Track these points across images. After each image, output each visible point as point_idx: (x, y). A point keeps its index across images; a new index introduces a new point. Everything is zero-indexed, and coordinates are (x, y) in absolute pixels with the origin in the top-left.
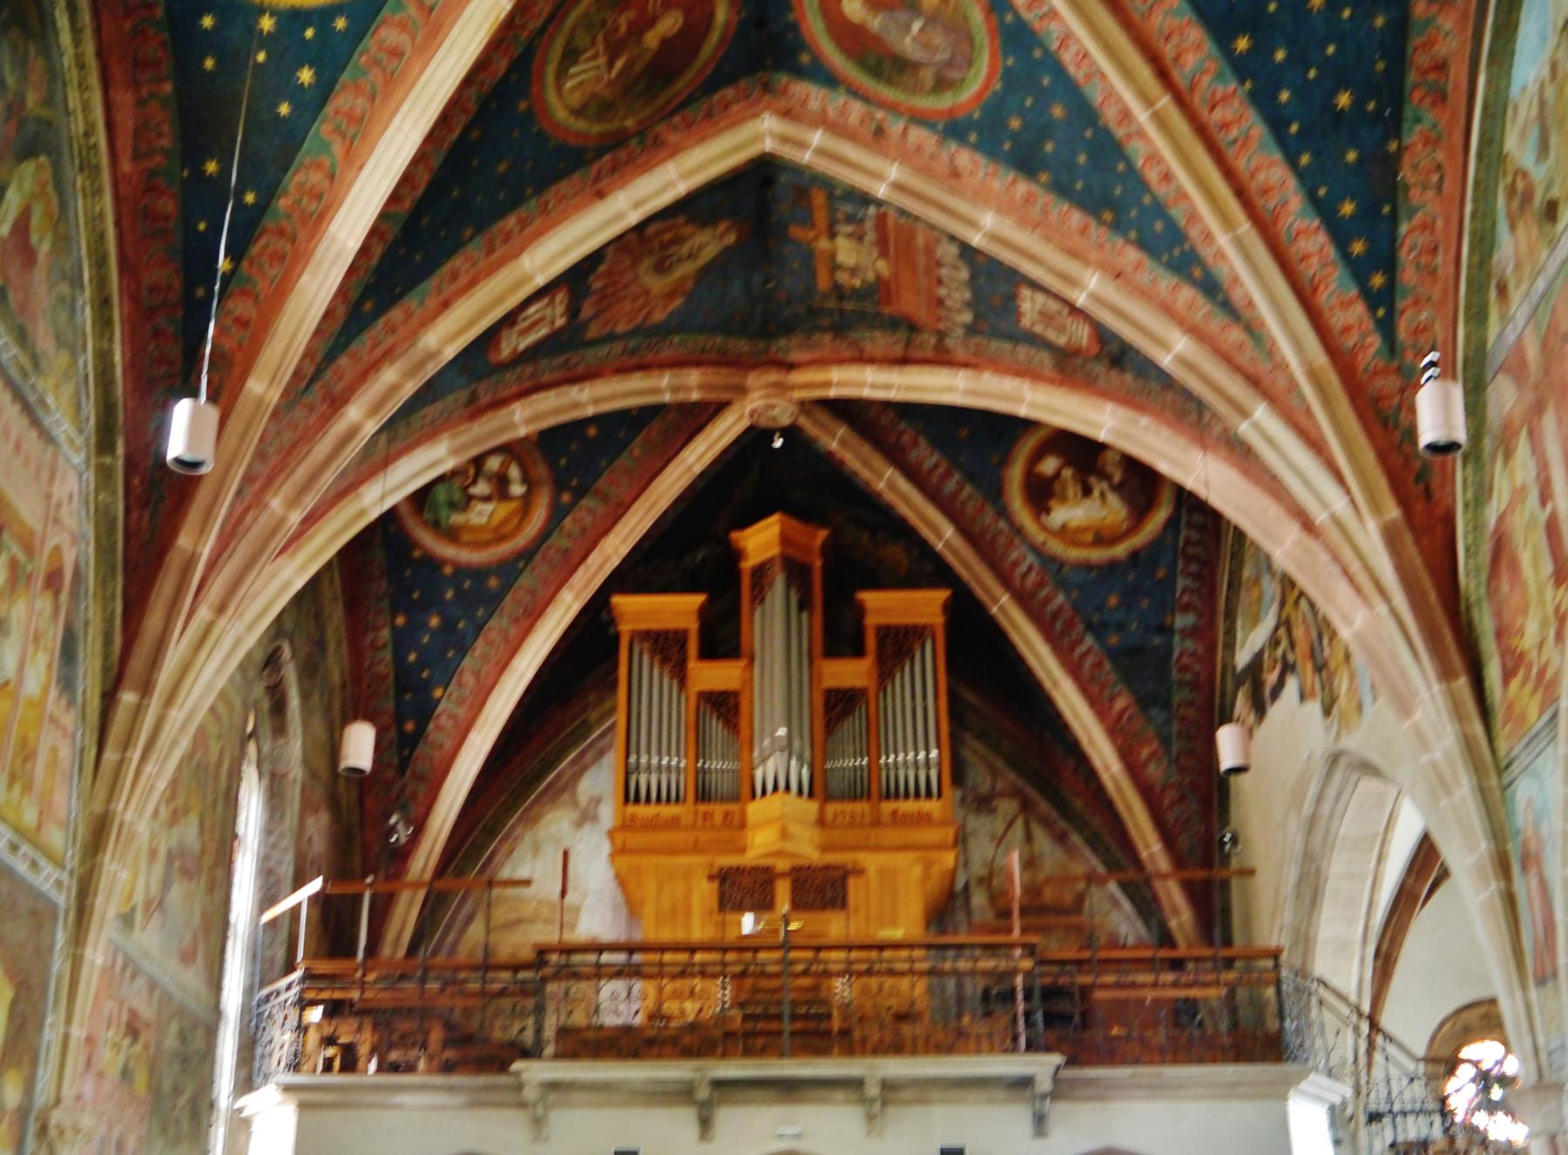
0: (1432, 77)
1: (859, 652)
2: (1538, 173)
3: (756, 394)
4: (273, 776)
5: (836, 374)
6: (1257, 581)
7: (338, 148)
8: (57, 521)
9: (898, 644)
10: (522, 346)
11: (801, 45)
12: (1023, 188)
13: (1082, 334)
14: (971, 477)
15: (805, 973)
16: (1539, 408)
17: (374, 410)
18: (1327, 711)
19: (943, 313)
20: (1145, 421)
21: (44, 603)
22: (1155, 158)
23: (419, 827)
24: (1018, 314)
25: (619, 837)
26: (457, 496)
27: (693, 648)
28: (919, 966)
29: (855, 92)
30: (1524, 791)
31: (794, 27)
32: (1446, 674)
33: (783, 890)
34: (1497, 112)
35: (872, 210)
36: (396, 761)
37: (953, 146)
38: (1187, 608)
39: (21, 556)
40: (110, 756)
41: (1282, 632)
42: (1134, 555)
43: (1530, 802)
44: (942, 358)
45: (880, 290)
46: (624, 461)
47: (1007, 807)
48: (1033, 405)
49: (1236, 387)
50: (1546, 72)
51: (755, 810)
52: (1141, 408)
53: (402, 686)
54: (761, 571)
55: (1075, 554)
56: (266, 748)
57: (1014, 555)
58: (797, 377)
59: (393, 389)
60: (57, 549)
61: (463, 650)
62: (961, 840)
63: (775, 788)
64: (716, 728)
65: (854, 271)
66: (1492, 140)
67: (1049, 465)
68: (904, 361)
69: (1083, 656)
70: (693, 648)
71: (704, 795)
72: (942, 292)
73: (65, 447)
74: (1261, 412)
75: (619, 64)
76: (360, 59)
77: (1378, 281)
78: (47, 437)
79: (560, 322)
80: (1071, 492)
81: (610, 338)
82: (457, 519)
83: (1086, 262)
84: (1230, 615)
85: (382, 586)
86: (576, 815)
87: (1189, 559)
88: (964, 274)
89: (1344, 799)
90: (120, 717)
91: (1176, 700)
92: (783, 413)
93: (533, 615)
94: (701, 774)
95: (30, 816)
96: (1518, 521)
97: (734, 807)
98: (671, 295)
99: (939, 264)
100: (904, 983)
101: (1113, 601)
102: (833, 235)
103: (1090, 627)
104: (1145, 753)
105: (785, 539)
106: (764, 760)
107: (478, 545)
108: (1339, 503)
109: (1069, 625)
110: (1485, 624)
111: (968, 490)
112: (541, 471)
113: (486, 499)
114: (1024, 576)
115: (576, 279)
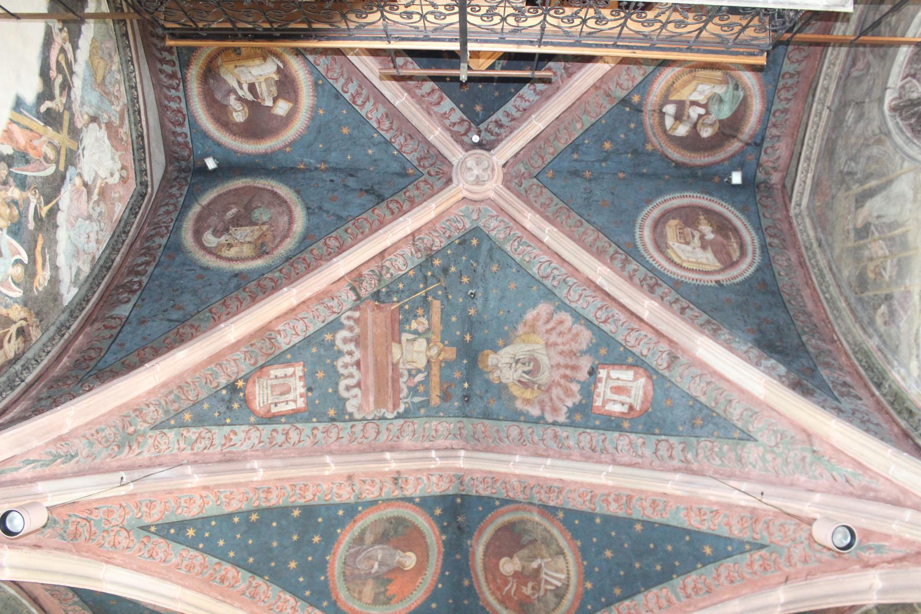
11: (438, 520)
13: (261, 396)
14: (338, 96)
26: (714, 108)
29: (410, 500)
31: (443, 530)
35: (402, 409)
44: (355, 278)
45: (396, 328)
46: (588, 121)
67: (282, 108)
80: (264, 86)
81: (578, 316)
82: (720, 90)
112: (649, 120)
113: (694, 103)
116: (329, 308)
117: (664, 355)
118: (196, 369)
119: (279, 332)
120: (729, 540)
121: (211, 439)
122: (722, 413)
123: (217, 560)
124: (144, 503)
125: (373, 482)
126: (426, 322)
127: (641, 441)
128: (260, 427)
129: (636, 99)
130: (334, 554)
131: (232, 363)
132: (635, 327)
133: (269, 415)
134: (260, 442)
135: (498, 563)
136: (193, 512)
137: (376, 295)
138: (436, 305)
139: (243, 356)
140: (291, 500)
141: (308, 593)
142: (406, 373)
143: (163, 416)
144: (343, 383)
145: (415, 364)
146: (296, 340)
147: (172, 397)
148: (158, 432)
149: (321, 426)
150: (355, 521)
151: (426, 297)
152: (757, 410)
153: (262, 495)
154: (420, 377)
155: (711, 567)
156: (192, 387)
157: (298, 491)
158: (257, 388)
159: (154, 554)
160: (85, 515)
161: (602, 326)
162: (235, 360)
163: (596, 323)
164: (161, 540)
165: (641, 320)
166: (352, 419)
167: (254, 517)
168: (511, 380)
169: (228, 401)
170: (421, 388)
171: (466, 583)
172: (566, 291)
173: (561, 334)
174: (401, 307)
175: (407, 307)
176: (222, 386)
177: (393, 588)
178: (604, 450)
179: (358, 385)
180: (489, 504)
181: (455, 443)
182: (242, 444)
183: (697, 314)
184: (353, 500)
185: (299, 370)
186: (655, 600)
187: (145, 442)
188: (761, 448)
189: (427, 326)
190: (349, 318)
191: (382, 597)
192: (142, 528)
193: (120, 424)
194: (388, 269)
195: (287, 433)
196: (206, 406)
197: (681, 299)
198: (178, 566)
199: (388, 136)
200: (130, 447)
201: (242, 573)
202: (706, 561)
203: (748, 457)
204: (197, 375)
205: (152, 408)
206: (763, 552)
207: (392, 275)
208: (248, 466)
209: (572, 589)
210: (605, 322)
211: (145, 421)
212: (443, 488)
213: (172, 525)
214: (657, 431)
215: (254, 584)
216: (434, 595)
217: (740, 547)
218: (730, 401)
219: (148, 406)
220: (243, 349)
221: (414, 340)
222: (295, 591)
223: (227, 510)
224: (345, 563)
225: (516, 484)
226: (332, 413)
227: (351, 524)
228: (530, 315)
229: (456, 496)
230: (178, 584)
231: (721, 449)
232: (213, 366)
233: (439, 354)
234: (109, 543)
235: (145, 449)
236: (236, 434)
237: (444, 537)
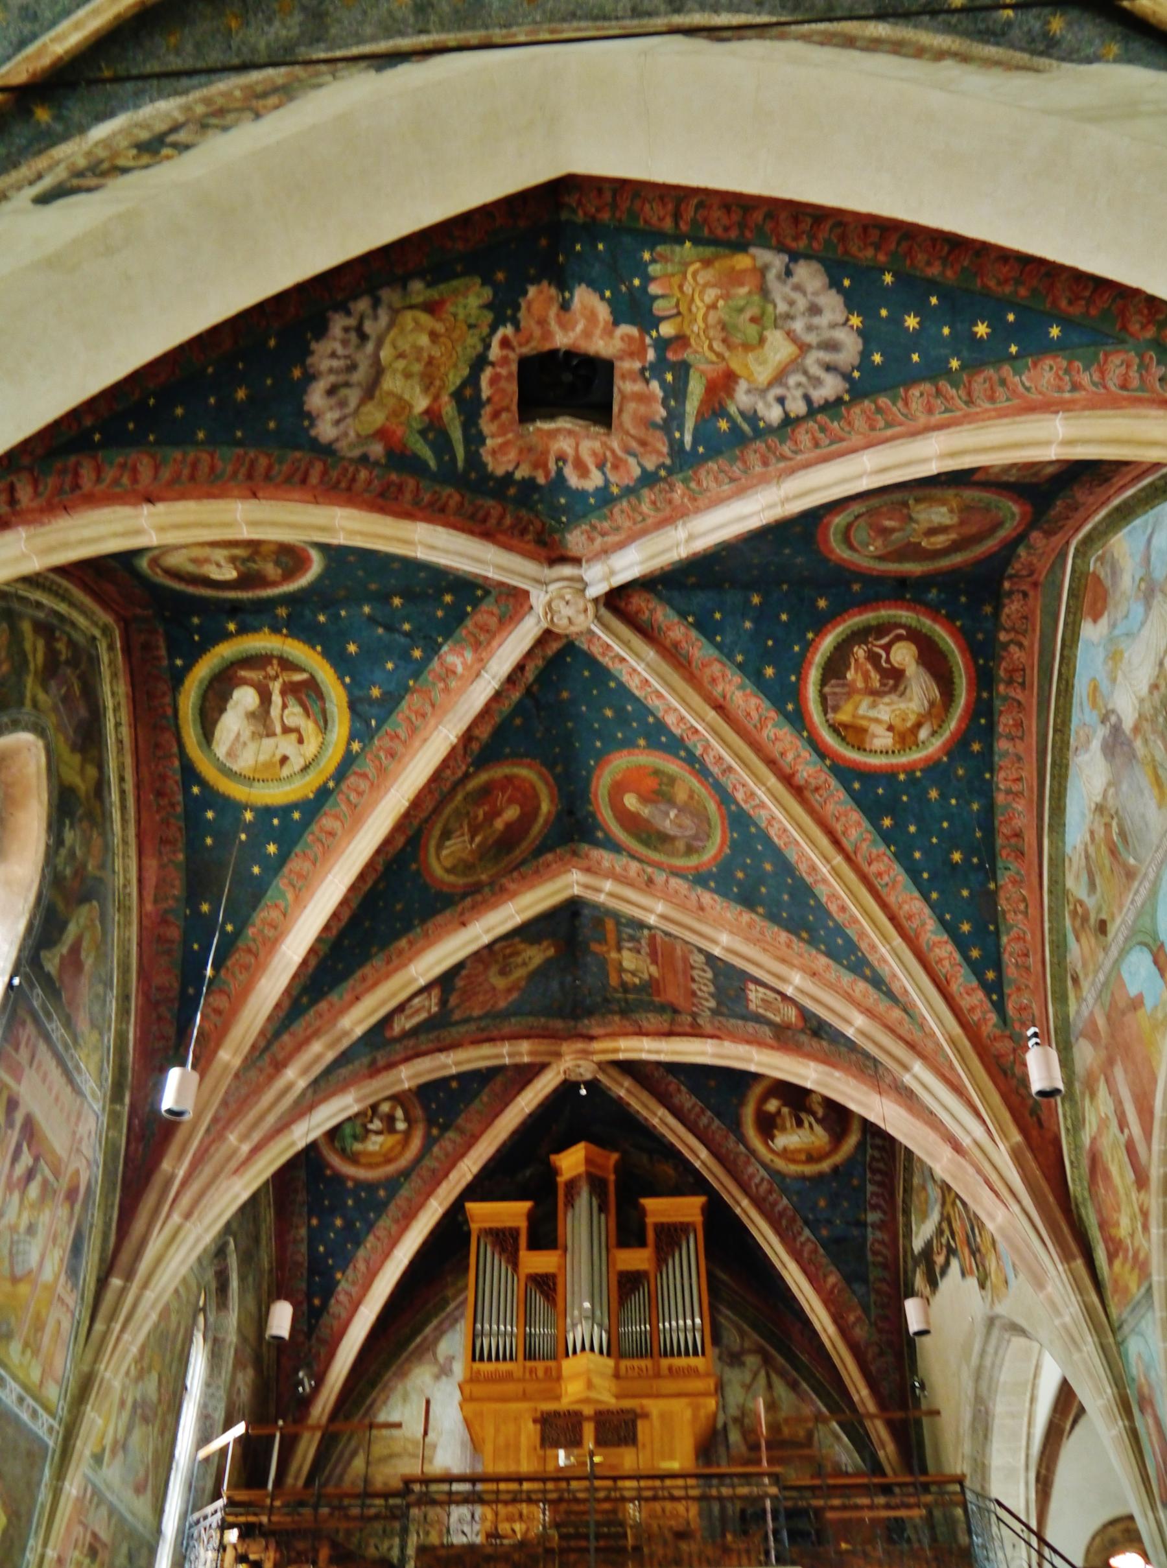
0: (1013, 841)
1: (642, 1244)
2: (1091, 902)
3: (568, 1058)
4: (216, 1340)
5: (623, 1043)
6: (924, 1188)
7: (290, 896)
8: (78, 1151)
9: (670, 1237)
10: (408, 1026)
11: (597, 826)
12: (746, 917)
13: (792, 1014)
14: (718, 1115)
15: (607, 1499)
16: (1110, 1062)
17: (305, 1071)
18: (982, 1286)
19: (695, 1001)
20: (837, 1074)
21: (63, 1212)
22: (834, 896)
23: (320, 1379)
24: (747, 1000)
25: (467, 1389)
26: (359, 1130)
27: (523, 1241)
28: (694, 1493)
29: (633, 856)
30: (1134, 1346)
31: (592, 815)
32: (1067, 1257)
33: (589, 1430)
34: (1058, 862)
36: (305, 1329)
37: (699, 890)
38: (875, 1207)
39: (51, 1178)
40: (99, 1327)
41: (945, 1225)
42: (836, 1169)
43: (1139, 1355)
44: (696, 1032)
45: (651, 986)
46: (477, 1105)
47: (752, 1361)
48: (759, 1064)
49: (900, 1050)
50: (1088, 837)
51: (569, 1366)
52: (834, 1066)
53: (312, 1271)
54: (571, 1185)
55: (793, 1169)
56: (211, 1319)
57: (751, 1170)
58: (596, 1046)
59: (319, 1057)
60: (77, 1172)
61: (358, 1243)
62: (720, 1388)
63: (583, 1348)
64: (539, 1300)
65: (634, 974)
66: (1057, 881)
67: (772, 1105)
68: (670, 1034)
69: (803, 1244)
70: (523, 1241)
71: (530, 1355)
72: (695, 986)
73: (90, 1098)
74: (918, 1067)
76: (308, 838)
77: (991, 975)
78: (78, 1091)
79: (434, 1009)
80: (788, 1125)
81: (466, 1021)
82: (358, 1147)
83: (792, 965)
84: (907, 1213)
85: (302, 1197)
86: (435, 1370)
87: (874, 1171)
88: (709, 975)
89: (1001, 1352)
90: (109, 1297)
91: (871, 1278)
92: (587, 1070)
93: (409, 1217)
94: (528, 1337)
95: (35, 1375)
96: (1105, 1144)
97: (552, 1364)
98: (509, 991)
99: (692, 968)
100: (680, 1507)
101: (822, 1203)
102: (619, 949)
103: (807, 1223)
104: (852, 1318)
105: (589, 1161)
106: (574, 1326)
107: (370, 1166)
108: (978, 1131)
109: (792, 1221)
110: (1091, 1219)
111: (717, 1122)
112: (418, 1112)
113: (378, 1133)
114: (757, 1186)
115: (446, 981)
129: (435, 1132)
177: (651, 783)
199: (670, 1078)
216: (601, 756)
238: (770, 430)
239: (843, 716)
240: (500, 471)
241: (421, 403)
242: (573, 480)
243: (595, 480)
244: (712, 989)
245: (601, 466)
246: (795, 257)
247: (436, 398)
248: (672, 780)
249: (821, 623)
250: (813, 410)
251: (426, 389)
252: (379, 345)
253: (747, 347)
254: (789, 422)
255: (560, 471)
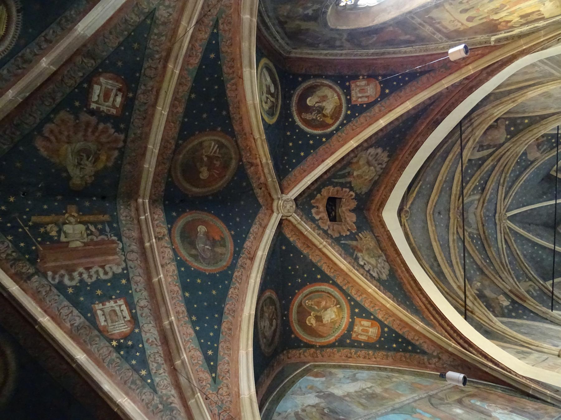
13: (121, 328)
29: (170, 230)
31: (184, 211)
75: (205, 159)
116: (47, 293)
117: (85, 61)
118: (110, 376)
119: (72, 325)
120: (209, 43)
121: (154, 354)
122: (132, 28)
123: (221, 335)
124: (201, 384)
125: (163, 252)
126: (50, 226)
127: (143, 87)
128: (141, 325)
130: (205, 270)
131: (101, 352)
132: (60, 78)
133: (133, 321)
134: (150, 323)
135: (203, 180)
136: (198, 354)
137: (33, 262)
138: (35, 219)
139: (94, 346)
140: (181, 299)
141: (226, 282)
142: (90, 237)
143: (147, 389)
144: (102, 276)
145: (83, 232)
146: (76, 312)
147: (133, 387)
148: (157, 389)
149: (134, 287)
150: (186, 260)
151: (29, 226)
152: (135, 3)
153: (181, 316)
154: (92, 228)
155: (222, 55)
156: (123, 375)
157: (175, 295)
158: (114, 332)
159: (226, 371)
160: (217, 417)
161: (58, 101)
162: (98, 351)
163: (54, 106)
164: (218, 369)
165: (55, 73)
166: (126, 268)
167: (194, 318)
168: (92, 168)
169: (129, 349)
170: (100, 226)
171: (211, 198)
172: (26, 126)
173: (61, 133)
174: (40, 243)
175: (39, 239)
176: (118, 355)
177: (217, 238)
178: (146, 111)
179: (103, 267)
180: (170, 185)
181: (133, 205)
182: (154, 334)
183: (51, 32)
184: (175, 263)
185: (98, 307)
186: (232, 92)
187: (166, 395)
188: (161, 7)
189: (53, 225)
190: (53, 279)
191: (222, 243)
192: (215, 382)
193: (159, 415)
194: (8, 255)
195: (142, 307)
196: (134, 362)
197: (36, 41)
198: (229, 355)
200: (171, 403)
201: (224, 320)
202: (218, 58)
203: (165, 17)
204: (114, 374)
205: (144, 397)
206: (220, 22)
207: (13, 252)
208: (168, 327)
209: (220, 139)
210: (54, 99)
211: (153, 399)
212: (160, 211)
213: (209, 365)
214: (138, 75)
215: (227, 312)
216: (217, 215)
217: (214, 36)
218: (126, 20)
219: (143, 400)
220: (89, 347)
221: (65, 233)
222: (227, 288)
223: (194, 335)
224: (209, 264)
225: (160, 168)
226: (124, 281)
227: (188, 263)
228: (44, 153)
229: (165, 205)
230: (238, 352)
231: (156, 34)
232: (105, 365)
233: (74, 216)
234: (228, 398)
235: (169, 393)
236: (148, 339)
237: (188, 210)
238: (358, 263)
239: (265, 309)
240: (323, 190)
241: (355, 174)
242: (313, 211)
243: (317, 217)
244: (89, 281)
245: (320, 219)
246: (388, 262)
247: (354, 177)
248: (224, 246)
249: (277, 294)
250: (368, 271)
251: (358, 176)
252: (375, 167)
253: (369, 254)
254: (362, 267)
255: (314, 207)
